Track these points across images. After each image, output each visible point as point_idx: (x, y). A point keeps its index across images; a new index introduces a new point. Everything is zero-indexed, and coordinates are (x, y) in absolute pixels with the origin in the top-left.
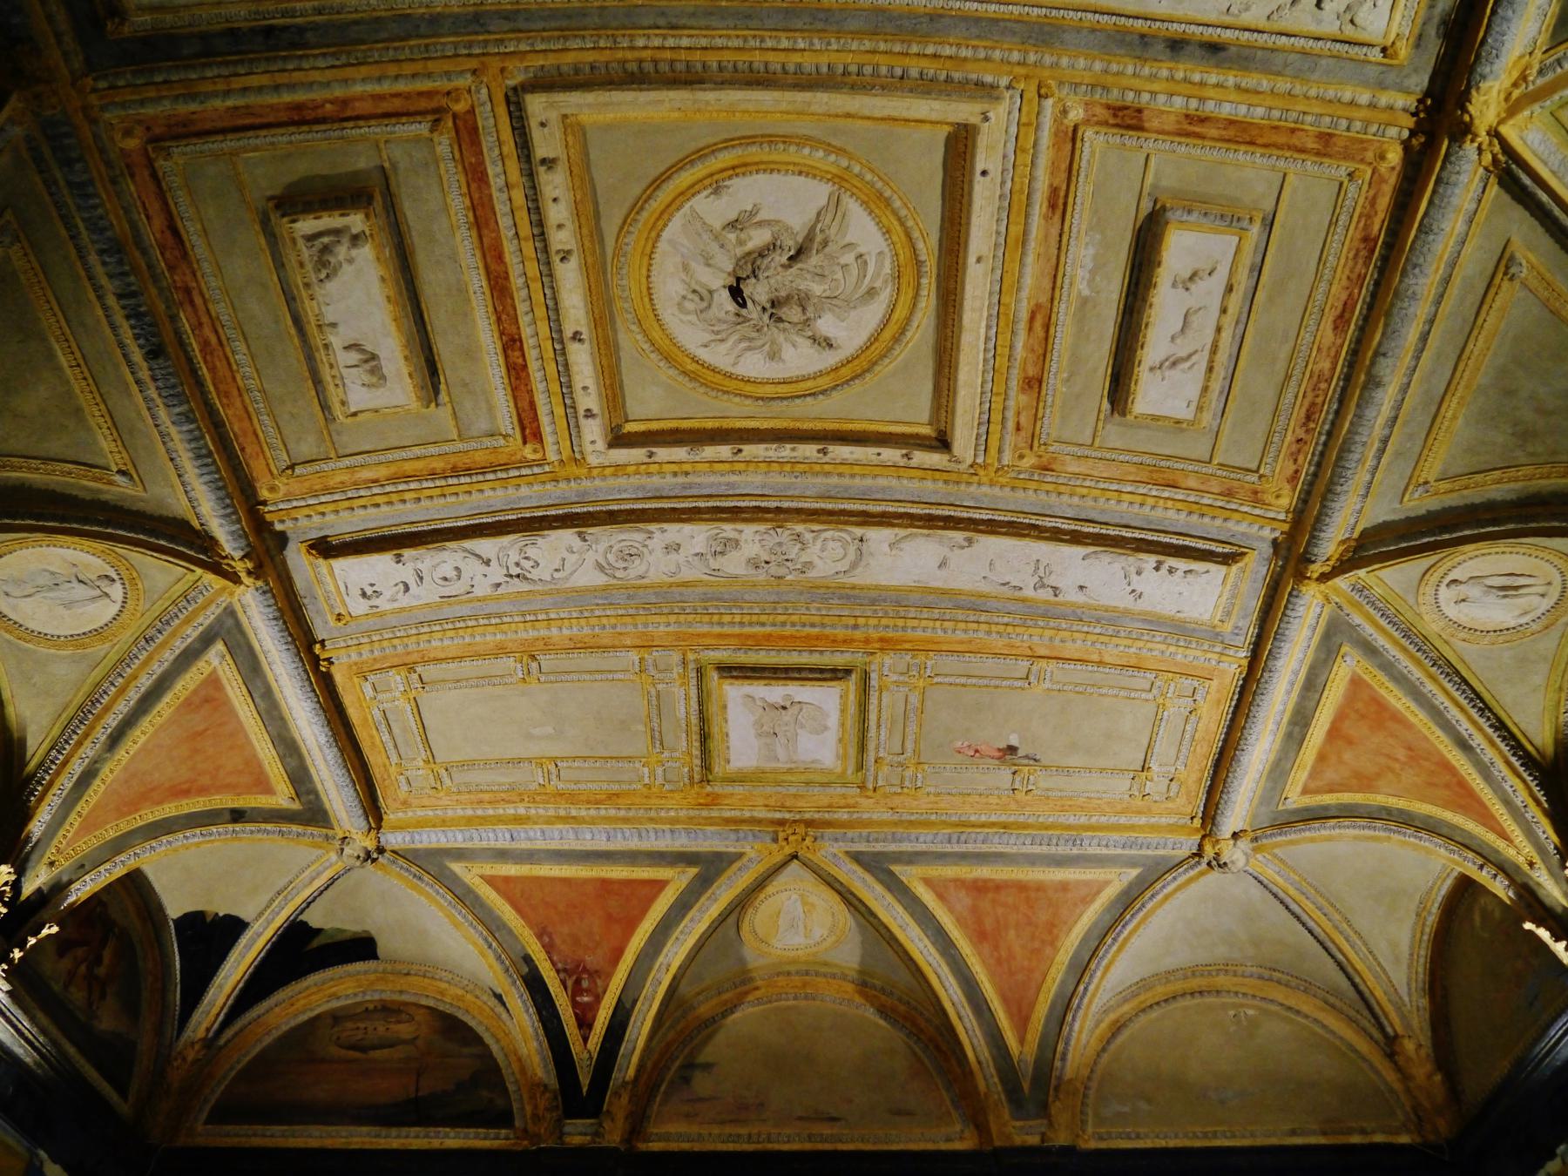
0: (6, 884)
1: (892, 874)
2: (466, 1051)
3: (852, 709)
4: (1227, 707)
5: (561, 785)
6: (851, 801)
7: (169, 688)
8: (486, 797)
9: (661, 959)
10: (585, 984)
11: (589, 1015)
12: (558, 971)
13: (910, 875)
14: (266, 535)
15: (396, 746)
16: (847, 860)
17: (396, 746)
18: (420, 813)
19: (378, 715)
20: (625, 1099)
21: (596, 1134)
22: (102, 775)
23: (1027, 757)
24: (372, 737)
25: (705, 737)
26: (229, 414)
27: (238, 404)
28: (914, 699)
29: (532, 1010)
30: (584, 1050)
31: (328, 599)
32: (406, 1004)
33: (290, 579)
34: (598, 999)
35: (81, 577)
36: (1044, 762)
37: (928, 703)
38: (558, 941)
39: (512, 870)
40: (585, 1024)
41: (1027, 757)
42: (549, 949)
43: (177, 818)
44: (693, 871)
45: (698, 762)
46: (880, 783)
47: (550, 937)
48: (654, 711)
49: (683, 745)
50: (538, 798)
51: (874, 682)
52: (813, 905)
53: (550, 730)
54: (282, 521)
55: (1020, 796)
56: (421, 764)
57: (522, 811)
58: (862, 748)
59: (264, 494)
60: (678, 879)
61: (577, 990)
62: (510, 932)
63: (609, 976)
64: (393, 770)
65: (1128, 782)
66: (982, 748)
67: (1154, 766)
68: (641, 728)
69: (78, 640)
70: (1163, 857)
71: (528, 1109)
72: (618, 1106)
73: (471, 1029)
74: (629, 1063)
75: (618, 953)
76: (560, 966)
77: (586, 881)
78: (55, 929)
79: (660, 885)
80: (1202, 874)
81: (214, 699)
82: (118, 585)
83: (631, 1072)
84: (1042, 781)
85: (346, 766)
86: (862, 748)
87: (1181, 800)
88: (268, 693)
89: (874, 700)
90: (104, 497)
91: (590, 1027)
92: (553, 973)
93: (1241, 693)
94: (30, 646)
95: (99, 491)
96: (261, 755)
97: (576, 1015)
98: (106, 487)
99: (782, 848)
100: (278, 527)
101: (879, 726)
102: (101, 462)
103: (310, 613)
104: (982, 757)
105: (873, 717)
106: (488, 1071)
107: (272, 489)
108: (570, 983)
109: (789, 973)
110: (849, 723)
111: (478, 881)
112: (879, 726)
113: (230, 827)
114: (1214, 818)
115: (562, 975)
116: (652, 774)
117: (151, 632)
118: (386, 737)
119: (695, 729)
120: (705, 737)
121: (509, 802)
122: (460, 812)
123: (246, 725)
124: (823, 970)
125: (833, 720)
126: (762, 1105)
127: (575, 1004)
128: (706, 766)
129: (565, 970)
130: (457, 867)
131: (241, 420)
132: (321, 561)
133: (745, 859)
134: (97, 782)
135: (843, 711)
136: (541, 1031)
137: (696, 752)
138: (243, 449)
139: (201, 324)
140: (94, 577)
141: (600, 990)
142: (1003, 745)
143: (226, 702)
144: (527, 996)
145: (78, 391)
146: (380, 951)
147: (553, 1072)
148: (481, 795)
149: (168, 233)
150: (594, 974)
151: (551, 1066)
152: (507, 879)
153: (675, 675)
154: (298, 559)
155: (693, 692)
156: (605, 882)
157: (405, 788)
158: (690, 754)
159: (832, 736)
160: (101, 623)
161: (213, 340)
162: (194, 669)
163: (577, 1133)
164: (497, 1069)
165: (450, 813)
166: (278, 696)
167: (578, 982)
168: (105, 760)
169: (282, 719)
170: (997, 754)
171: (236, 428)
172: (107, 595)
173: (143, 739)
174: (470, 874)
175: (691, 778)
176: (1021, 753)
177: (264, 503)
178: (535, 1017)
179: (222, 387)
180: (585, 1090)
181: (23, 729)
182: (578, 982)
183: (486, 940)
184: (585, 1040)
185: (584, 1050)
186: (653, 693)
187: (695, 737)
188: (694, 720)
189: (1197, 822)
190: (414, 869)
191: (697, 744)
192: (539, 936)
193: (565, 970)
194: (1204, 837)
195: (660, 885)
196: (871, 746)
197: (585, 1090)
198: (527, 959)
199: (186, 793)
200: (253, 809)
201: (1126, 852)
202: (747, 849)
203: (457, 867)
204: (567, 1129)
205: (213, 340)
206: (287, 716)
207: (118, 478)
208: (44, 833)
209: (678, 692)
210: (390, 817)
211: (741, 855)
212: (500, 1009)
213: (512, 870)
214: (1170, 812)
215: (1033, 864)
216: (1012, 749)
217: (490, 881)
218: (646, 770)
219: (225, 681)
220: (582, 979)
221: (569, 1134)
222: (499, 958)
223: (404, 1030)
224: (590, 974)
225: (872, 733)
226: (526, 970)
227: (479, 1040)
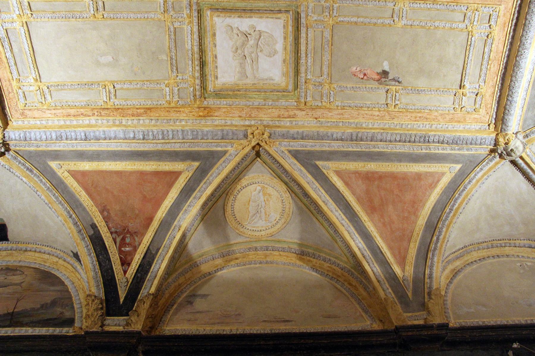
1: (317, 167)
2: (52, 288)
3: (291, 38)
4: (509, 28)
5: (117, 102)
6: (291, 113)
8: (72, 111)
9: (175, 223)
10: (128, 240)
11: (129, 258)
12: (111, 233)
13: (329, 168)
15: (16, 64)
16: (290, 156)
17: (16, 64)
18: (32, 122)
20: (147, 305)
21: (128, 324)
23: (394, 80)
25: (203, 64)
28: (327, 34)
29: (93, 254)
30: (123, 278)
32: (21, 267)
34: (135, 249)
36: (405, 83)
37: (335, 38)
38: (112, 214)
39: (86, 166)
40: (125, 263)
41: (394, 80)
42: (107, 219)
44: (196, 164)
45: (198, 82)
46: (309, 99)
47: (108, 212)
48: (173, 44)
49: (190, 70)
50: (103, 113)
51: (303, 20)
52: (269, 195)
53: (110, 58)
55: (392, 108)
56: (33, 81)
57: (93, 122)
58: (297, 72)
60: (186, 169)
61: (123, 243)
62: (84, 209)
63: (143, 235)
64: (14, 83)
65: (452, 97)
66: (368, 72)
67: (467, 84)
68: (164, 57)
70: (473, 156)
71: (85, 311)
72: (143, 308)
73: (58, 278)
74: (151, 287)
75: (150, 220)
76: (113, 230)
77: (131, 173)
79: (176, 175)
80: (497, 163)
83: (153, 290)
84: (405, 100)
86: (297, 72)
87: (482, 111)
89: (303, 35)
91: (129, 264)
92: (109, 234)
93: (519, 12)
97: (121, 258)
99: (250, 141)
101: (306, 56)
104: (369, 79)
105: (303, 48)
106: (65, 298)
108: (118, 240)
109: (256, 249)
110: (289, 48)
111: (66, 174)
112: (306, 56)
114: (503, 119)
115: (114, 235)
116: (172, 92)
118: (9, 54)
119: (197, 56)
120: (203, 64)
121: (86, 115)
122: (56, 123)
124: (277, 245)
125: (279, 46)
126: (239, 315)
127: (120, 252)
128: (203, 87)
129: (116, 232)
130: (53, 164)
133: (227, 155)
135: (285, 38)
136: (97, 267)
137: (197, 74)
141: (137, 243)
142: (380, 70)
144: (91, 247)
146: (10, 236)
147: (102, 290)
148: (69, 111)
150: (133, 234)
151: (102, 286)
152: (84, 174)
153: (185, 16)
155: (195, 29)
156: (142, 173)
157: (22, 100)
158: (194, 77)
159: (279, 58)
163: (115, 324)
164: (70, 298)
165: (50, 123)
167: (123, 239)
170: (377, 77)
174: (61, 169)
175: (195, 96)
176: (391, 76)
178: (95, 259)
180: (122, 300)
182: (123, 239)
183: (69, 212)
184: (125, 272)
185: (123, 278)
186: (172, 29)
187: (197, 63)
188: (196, 49)
189: (492, 126)
190: (28, 165)
191: (198, 68)
192: (102, 212)
193: (116, 232)
194: (497, 135)
195: (176, 175)
196: (302, 69)
197: (122, 300)
198: (94, 226)
201: (453, 152)
202: (229, 148)
203: (53, 164)
204: (106, 322)
209: (187, 28)
210: (13, 123)
211: (225, 152)
212: (77, 264)
213: (86, 166)
214: (476, 121)
215: (400, 161)
216: (385, 73)
217: (74, 174)
218: (167, 89)
220: (125, 236)
221: (109, 325)
222: (75, 224)
223: (17, 279)
224: (131, 235)
225: (303, 61)
226: (92, 232)
227: (62, 283)
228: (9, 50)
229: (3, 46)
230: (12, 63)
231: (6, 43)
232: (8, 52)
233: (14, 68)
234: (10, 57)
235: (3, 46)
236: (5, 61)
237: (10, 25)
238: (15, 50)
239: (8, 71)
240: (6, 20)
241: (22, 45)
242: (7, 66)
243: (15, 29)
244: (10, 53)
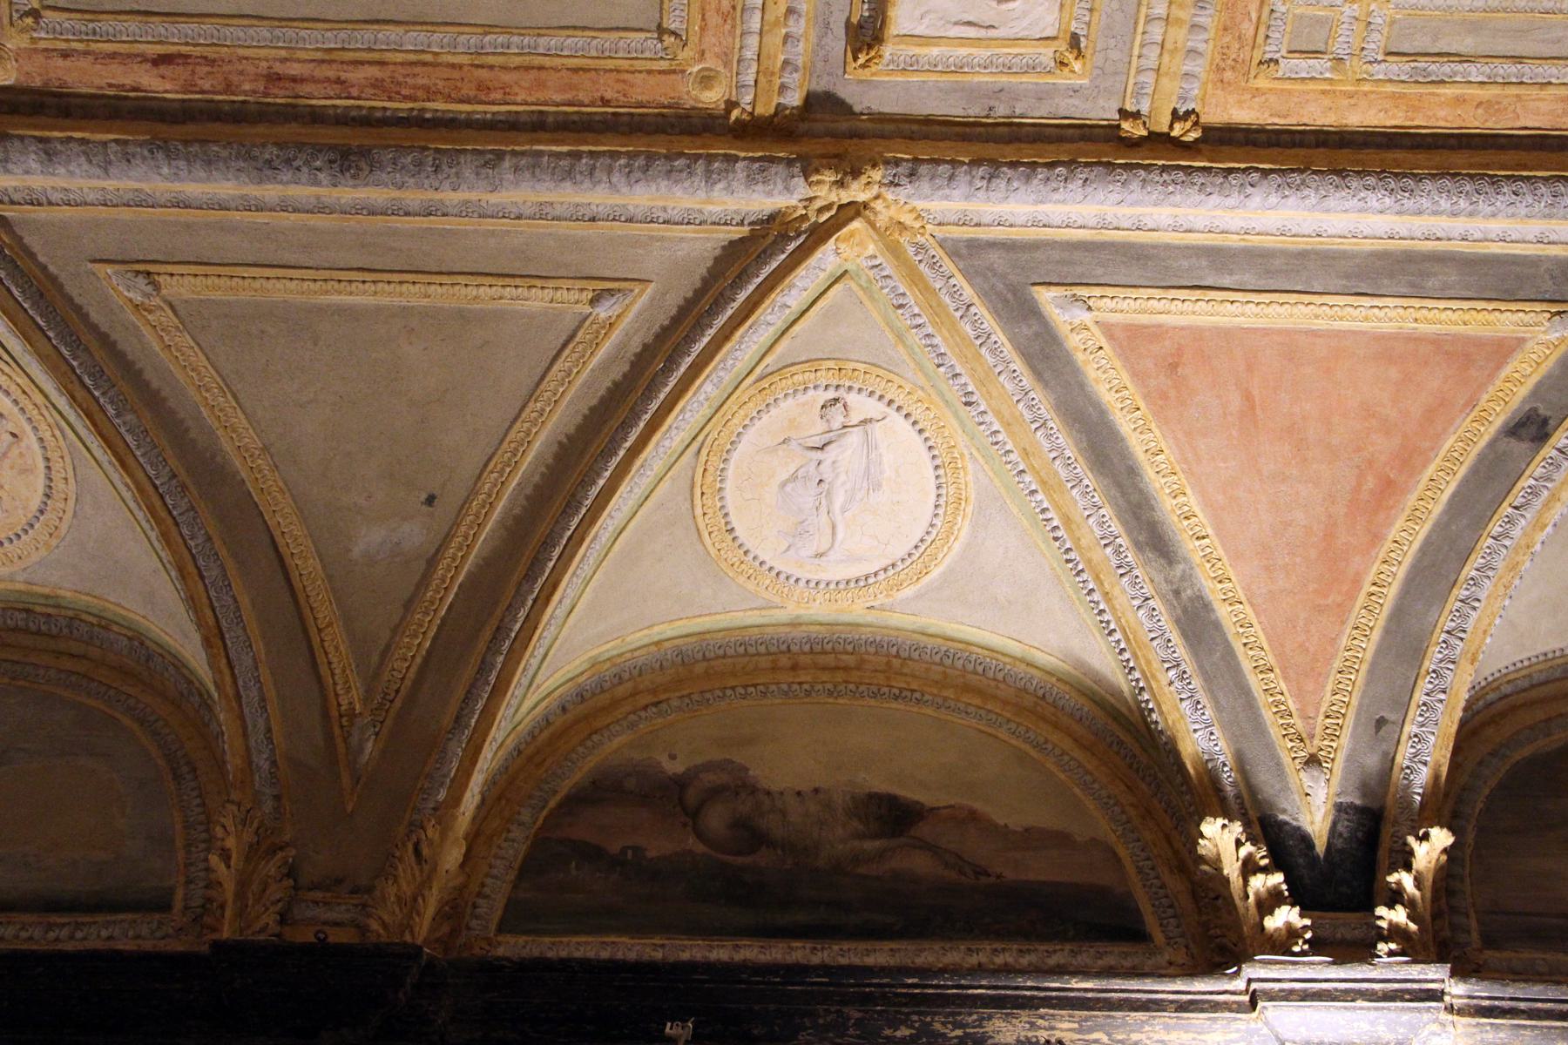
0: (1239, 844)
7: (1103, 413)
14: (803, 127)
15: (1518, 59)
17: (1518, 59)
19: (1397, 68)
22: (1213, 592)
24: (1460, 100)
26: (524, 99)
27: (507, 77)
31: (1008, 69)
33: (928, 121)
35: (818, 442)
43: (1441, 527)
54: (783, 88)
59: (712, 97)
69: (947, 502)
78: (1441, 838)
81: (1180, 352)
82: (852, 398)
85: (1494, 181)
88: (1218, 256)
90: (635, 346)
94: (935, 573)
95: (621, 346)
96: (1388, 327)
98: (616, 335)
100: (794, 99)
102: (569, 324)
103: (1035, 112)
107: (706, 80)
113: (1548, 451)
117: (955, 396)
118: (1475, 72)
123: (1281, 324)
131: (541, 85)
132: (888, 50)
134: (1223, 612)
138: (605, 102)
139: (339, 81)
140: (821, 426)
143: (1197, 333)
145: (425, 302)
149: (163, 69)
154: (878, 87)
160: (926, 455)
161: (374, 71)
162: (1080, 357)
166: (1233, 241)
168: (1187, 577)
169: (1303, 255)
171: (558, 98)
172: (864, 422)
173: (1192, 501)
177: (731, 105)
179: (468, 90)
181: (1080, 664)
199: (1389, 490)
200: (1536, 393)
205: (374, 71)
206: (1302, 244)
207: (603, 312)
208: (1233, 738)
219: (1144, 319)
228: (1460, 67)
229: (1443, 82)
230: (1509, 70)
231: (1433, 67)
232: (1466, 74)
233: (1528, 71)
234: (1486, 69)
235: (1443, 82)
236: (1494, 91)
237: (1375, 36)
238: (1466, 44)
239: (1534, 92)
240: (1357, 44)
241: (1456, 16)
242: (1513, 90)
243: (1393, 22)
244: (1472, 68)
